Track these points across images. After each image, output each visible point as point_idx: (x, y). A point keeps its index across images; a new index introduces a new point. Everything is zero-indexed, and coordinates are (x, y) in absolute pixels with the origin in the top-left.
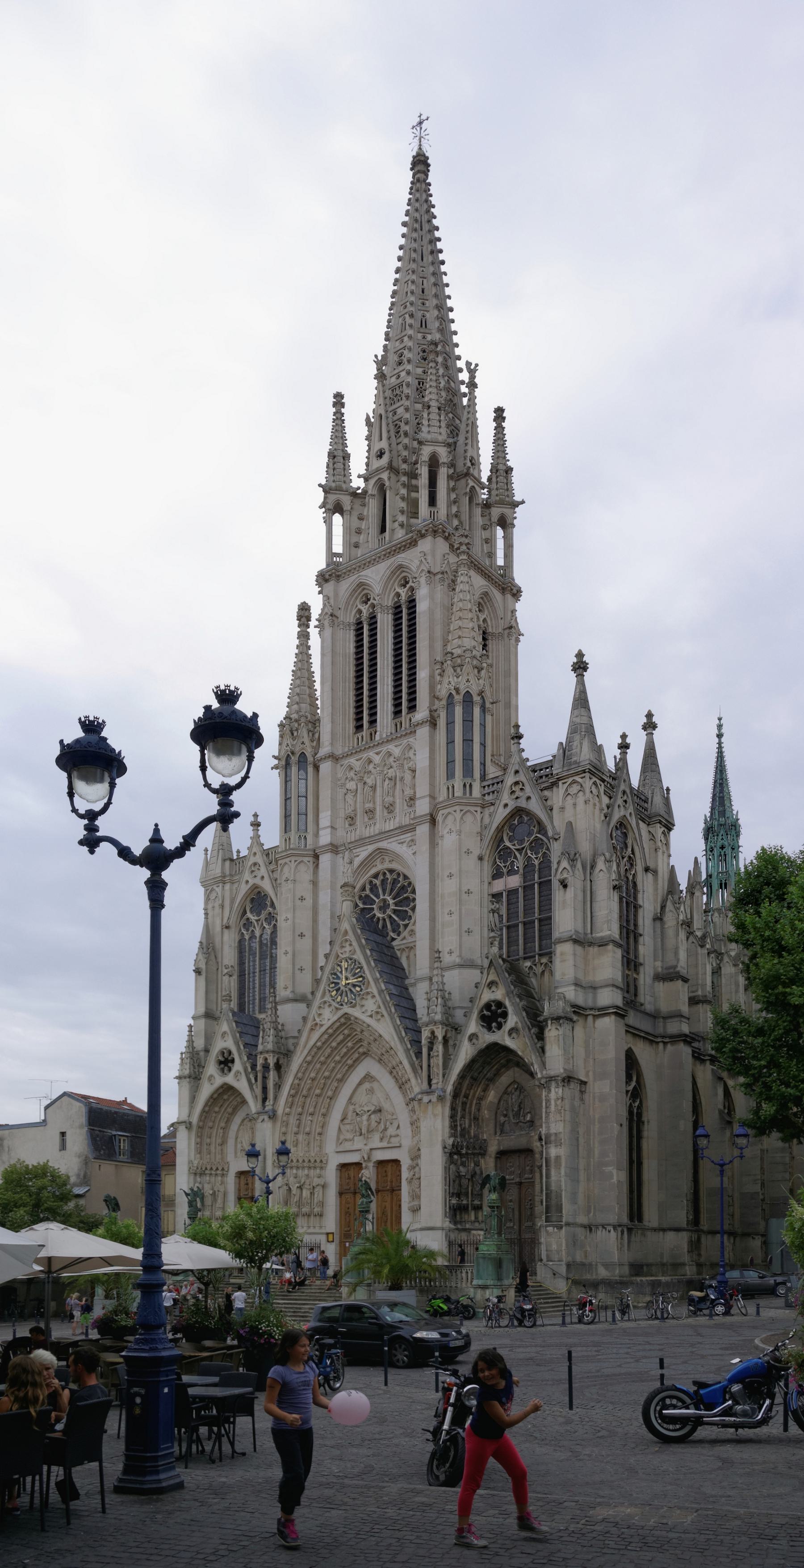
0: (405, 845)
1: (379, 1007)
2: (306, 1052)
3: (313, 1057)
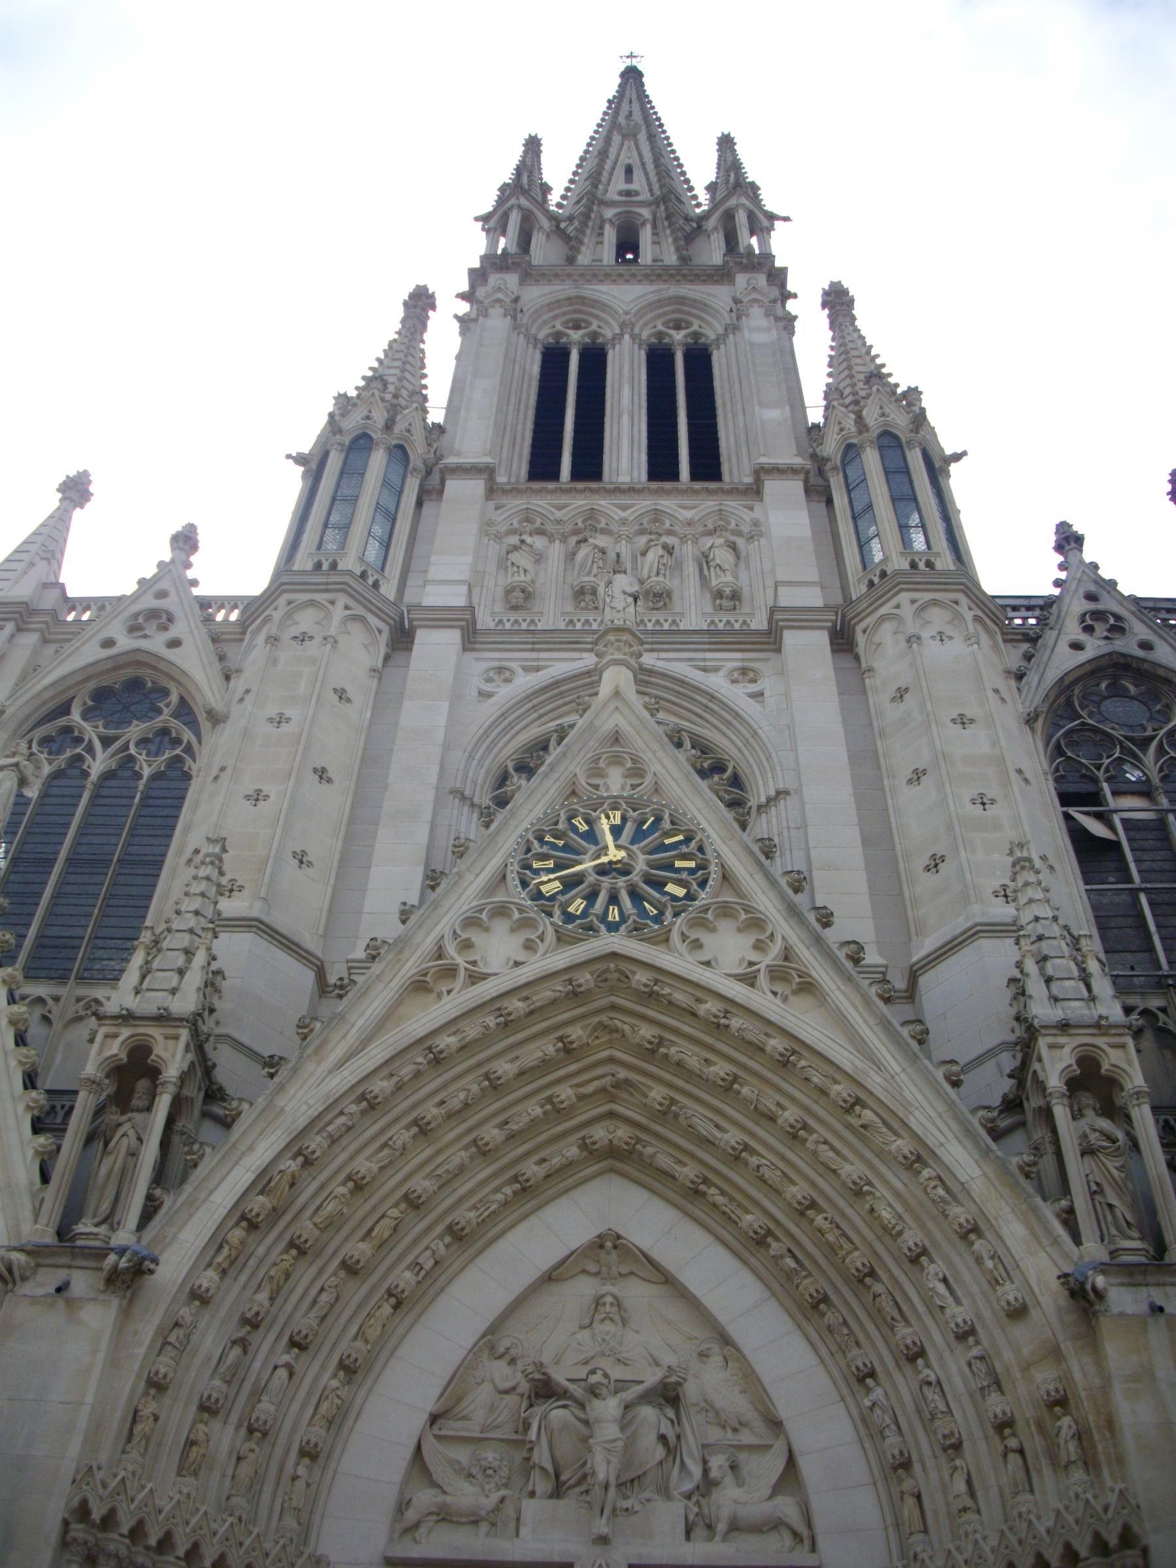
0: (721, 673)
1: (787, 954)
2: (377, 1054)
3: (399, 1087)
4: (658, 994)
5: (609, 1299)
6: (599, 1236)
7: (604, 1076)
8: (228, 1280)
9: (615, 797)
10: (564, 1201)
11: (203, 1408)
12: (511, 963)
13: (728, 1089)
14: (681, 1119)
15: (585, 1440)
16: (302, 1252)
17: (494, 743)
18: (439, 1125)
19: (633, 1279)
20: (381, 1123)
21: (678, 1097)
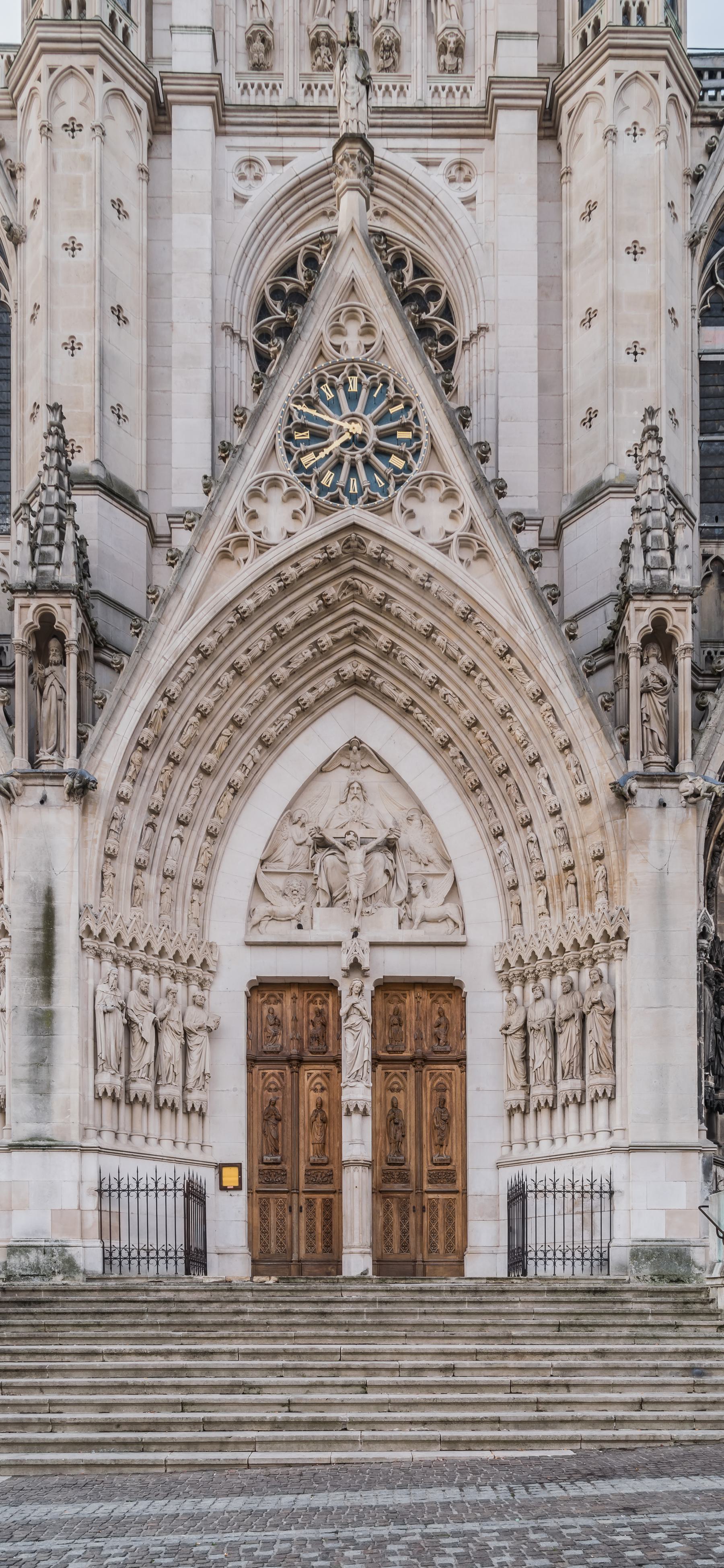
4: (384, 559)
5: (356, 785)
6: (349, 742)
7: (349, 625)
8: (137, 786)
9: (353, 361)
10: (327, 716)
11: (138, 866)
12: (285, 534)
13: (428, 637)
14: (399, 658)
15: (346, 873)
16: (177, 764)
17: (252, 264)
18: (248, 668)
19: (369, 769)
20: (213, 668)
21: (397, 641)
